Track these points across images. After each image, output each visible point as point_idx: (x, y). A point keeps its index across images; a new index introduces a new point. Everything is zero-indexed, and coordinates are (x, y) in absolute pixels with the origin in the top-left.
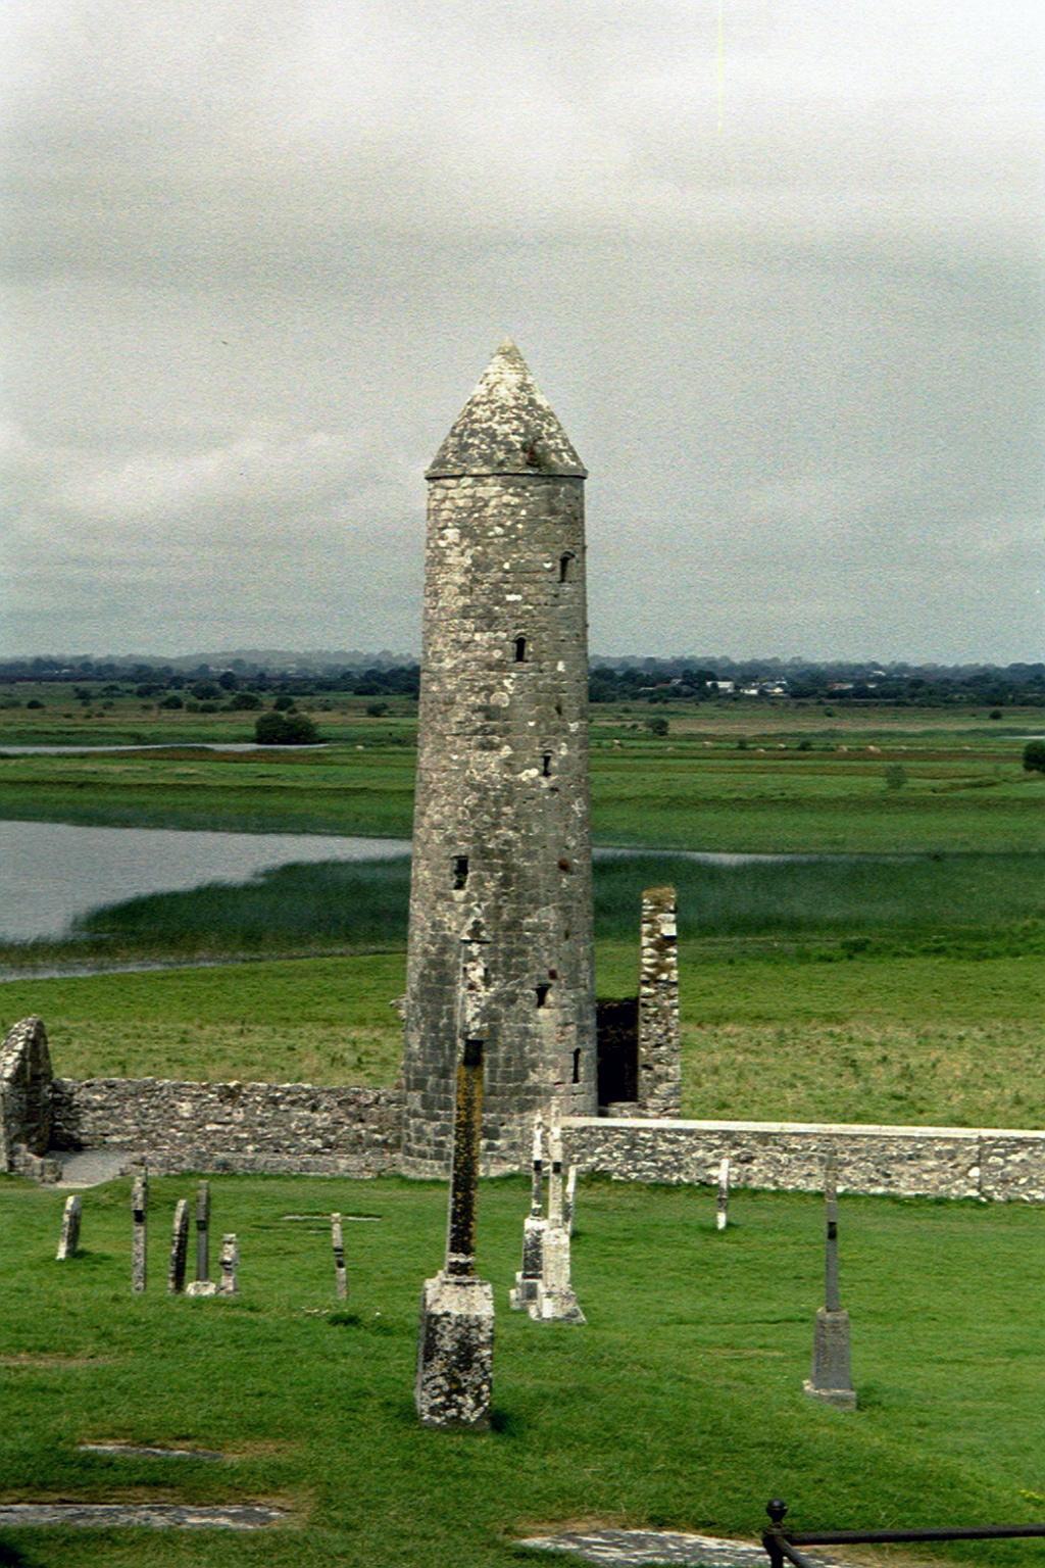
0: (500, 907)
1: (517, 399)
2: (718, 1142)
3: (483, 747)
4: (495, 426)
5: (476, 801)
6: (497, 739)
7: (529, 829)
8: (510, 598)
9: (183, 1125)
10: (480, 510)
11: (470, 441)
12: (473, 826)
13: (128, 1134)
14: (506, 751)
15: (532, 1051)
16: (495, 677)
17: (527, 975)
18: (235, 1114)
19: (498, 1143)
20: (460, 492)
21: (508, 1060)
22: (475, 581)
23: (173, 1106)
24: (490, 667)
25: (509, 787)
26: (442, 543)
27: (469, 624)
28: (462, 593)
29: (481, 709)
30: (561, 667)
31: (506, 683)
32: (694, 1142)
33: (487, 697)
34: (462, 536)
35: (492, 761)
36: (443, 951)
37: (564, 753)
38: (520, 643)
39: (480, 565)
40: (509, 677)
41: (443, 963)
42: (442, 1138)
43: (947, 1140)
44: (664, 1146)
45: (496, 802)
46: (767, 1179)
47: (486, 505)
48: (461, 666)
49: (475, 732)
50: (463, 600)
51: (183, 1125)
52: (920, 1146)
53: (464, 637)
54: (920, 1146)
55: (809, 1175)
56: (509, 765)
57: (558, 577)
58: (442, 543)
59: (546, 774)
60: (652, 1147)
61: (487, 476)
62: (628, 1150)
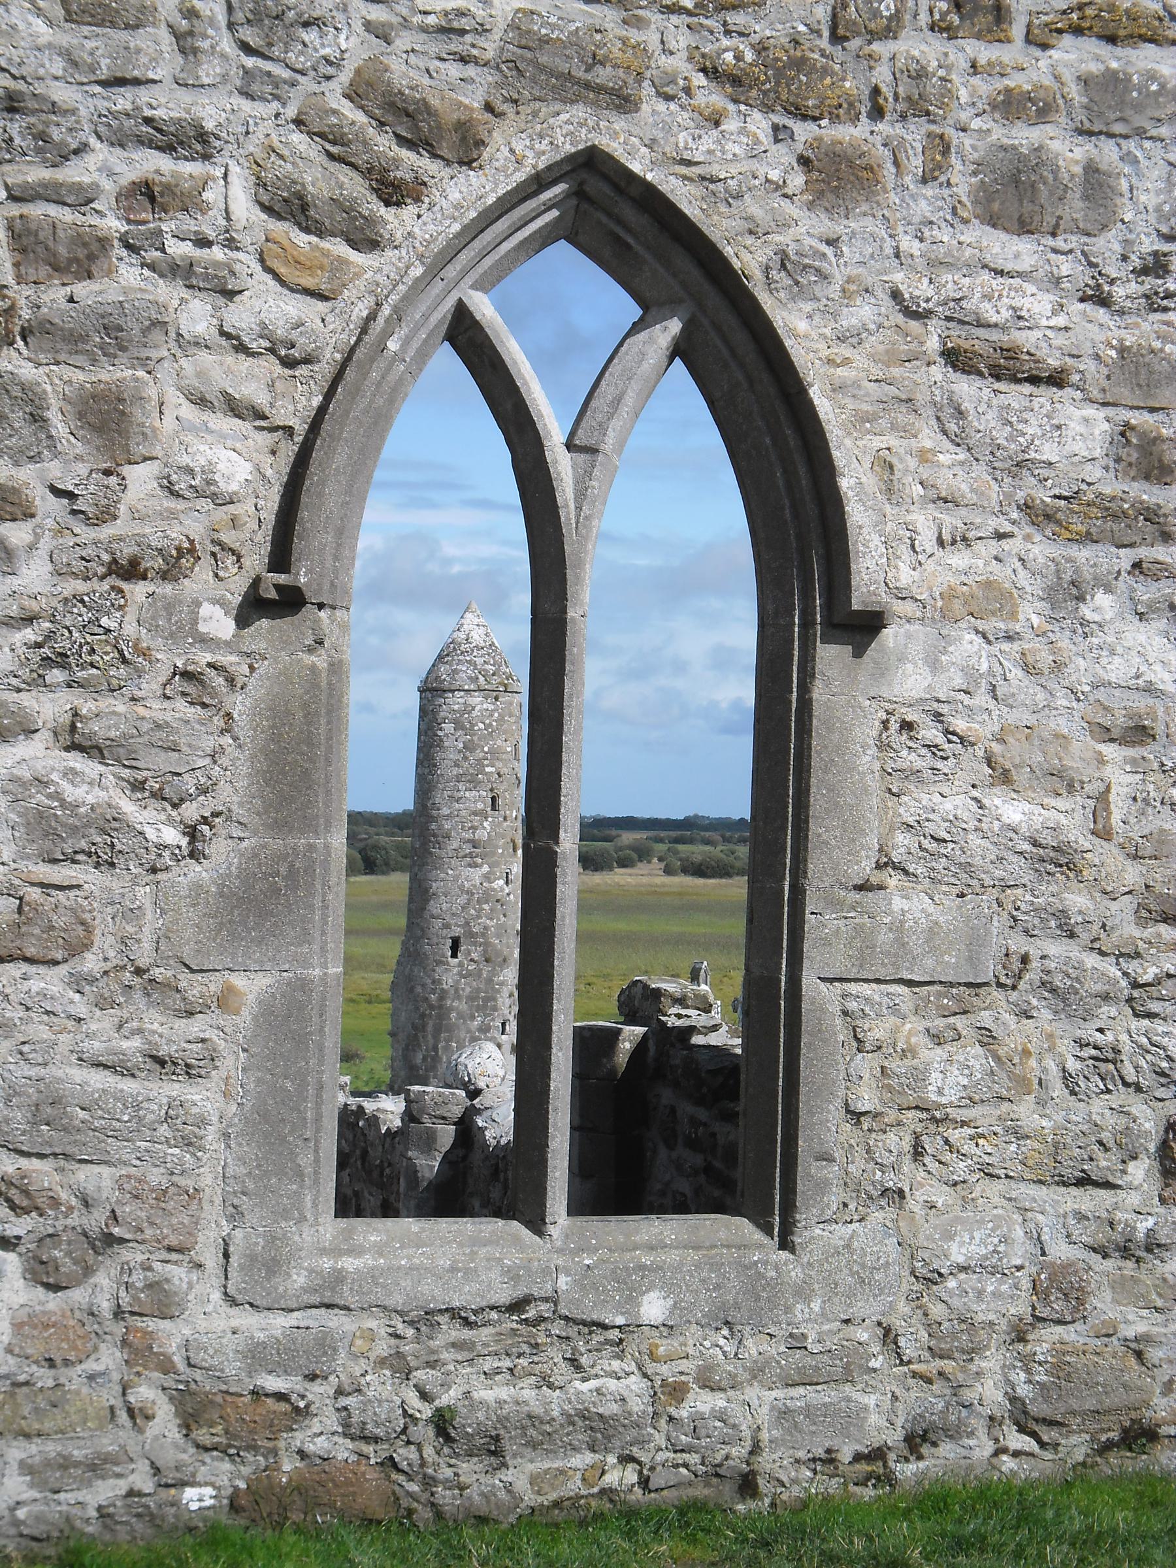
3: (470, 866)
8: (488, 769)
10: (469, 713)
14: (486, 868)
24: (475, 814)
25: (486, 893)
27: (461, 786)
28: (456, 765)
29: (469, 841)
31: (485, 824)
39: (469, 747)
41: (441, 1007)
47: (473, 709)
49: (465, 856)
50: (456, 771)
58: (440, 733)
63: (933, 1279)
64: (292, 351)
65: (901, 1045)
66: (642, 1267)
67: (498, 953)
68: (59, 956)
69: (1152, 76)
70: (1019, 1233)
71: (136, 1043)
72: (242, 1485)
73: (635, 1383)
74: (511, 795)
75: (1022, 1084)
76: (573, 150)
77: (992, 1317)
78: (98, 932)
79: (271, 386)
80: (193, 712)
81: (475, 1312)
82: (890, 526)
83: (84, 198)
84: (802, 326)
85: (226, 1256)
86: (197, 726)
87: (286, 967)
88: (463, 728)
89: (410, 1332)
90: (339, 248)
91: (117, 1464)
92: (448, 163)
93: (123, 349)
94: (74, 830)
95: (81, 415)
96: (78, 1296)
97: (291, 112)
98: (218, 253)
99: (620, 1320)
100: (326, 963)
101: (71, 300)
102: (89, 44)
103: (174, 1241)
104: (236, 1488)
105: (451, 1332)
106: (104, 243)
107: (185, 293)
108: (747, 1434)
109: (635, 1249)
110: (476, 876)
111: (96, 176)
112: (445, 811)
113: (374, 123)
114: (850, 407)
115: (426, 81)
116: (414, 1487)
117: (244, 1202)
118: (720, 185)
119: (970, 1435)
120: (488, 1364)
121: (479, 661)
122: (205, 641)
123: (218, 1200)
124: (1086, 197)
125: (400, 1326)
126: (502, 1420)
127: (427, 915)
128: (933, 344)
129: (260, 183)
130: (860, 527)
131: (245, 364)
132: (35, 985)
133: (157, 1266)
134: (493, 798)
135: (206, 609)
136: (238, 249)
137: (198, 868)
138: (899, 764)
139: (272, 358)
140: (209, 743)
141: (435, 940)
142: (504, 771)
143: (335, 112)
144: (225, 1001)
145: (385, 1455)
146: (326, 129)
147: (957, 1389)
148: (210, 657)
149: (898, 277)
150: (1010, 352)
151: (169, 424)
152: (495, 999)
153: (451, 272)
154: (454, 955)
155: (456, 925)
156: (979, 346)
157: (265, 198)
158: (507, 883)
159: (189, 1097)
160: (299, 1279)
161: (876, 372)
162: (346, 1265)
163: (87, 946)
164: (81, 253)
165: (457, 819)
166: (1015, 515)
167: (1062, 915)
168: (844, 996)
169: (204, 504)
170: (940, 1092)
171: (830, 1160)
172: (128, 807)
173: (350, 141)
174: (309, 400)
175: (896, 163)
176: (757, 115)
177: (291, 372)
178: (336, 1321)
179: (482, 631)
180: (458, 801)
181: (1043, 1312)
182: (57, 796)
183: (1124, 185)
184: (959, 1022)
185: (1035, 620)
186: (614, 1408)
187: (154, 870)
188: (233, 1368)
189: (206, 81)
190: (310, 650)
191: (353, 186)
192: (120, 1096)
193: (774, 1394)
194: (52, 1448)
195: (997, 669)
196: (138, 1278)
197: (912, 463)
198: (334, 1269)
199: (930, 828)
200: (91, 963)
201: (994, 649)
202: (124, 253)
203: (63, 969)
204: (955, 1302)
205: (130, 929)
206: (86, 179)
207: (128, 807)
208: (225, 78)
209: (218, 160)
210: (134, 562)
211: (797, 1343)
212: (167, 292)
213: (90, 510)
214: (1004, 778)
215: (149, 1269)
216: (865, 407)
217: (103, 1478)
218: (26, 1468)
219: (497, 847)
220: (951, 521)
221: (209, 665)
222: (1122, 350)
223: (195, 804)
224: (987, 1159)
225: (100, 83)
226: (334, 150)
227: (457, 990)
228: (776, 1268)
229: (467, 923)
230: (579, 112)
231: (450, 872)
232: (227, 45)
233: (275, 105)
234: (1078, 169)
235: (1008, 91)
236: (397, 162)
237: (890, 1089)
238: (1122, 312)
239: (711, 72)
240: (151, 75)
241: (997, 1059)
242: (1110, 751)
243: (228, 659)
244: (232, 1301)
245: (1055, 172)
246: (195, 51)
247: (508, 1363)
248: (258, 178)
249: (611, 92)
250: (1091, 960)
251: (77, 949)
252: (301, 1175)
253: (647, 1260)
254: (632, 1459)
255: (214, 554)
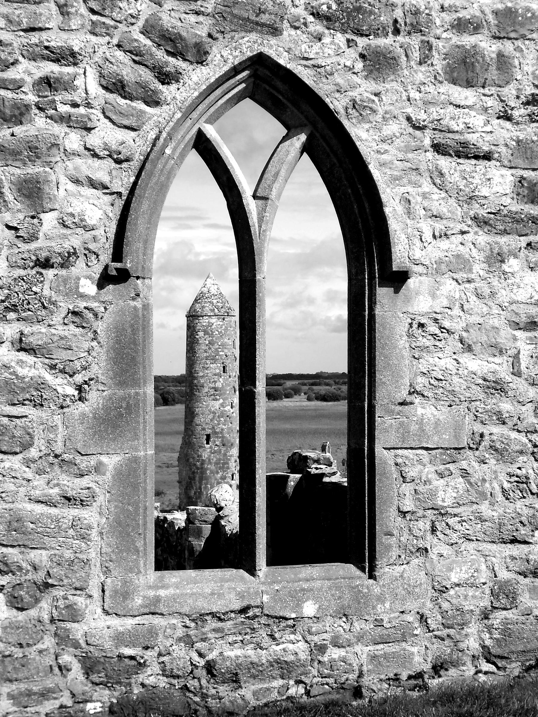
3: (214, 400)
6: (218, 397)
8: (221, 353)
10: (211, 326)
14: (221, 401)
24: (215, 375)
25: (222, 412)
27: (208, 362)
29: (213, 388)
31: (221, 379)
39: (211, 343)
41: (202, 468)
45: (218, 417)
49: (211, 395)
50: (205, 354)
58: (197, 337)
63: (443, 590)
64: (120, 156)
65: (424, 478)
66: (303, 590)
67: (229, 441)
68: (18, 451)
69: (528, 10)
70: (483, 567)
71: (56, 490)
72: (115, 701)
73: (302, 645)
74: (232, 365)
75: (483, 495)
76: (251, 55)
77: (472, 608)
78: (36, 438)
79: (110, 173)
80: (78, 331)
81: (224, 614)
82: (410, 230)
83: (17, 86)
84: (364, 135)
85: (103, 591)
86: (80, 338)
87: (127, 451)
88: (208, 334)
89: (193, 625)
90: (140, 105)
91: (54, 693)
92: (191, 63)
93: (38, 158)
94: (23, 389)
95: (19, 190)
96: (33, 613)
97: (115, 41)
98: (82, 110)
99: (293, 616)
100: (146, 449)
101: (13, 135)
102: (17, 12)
103: (78, 585)
104: (112, 703)
105: (212, 624)
106: (27, 107)
107: (67, 130)
108: (356, 668)
109: (299, 581)
110: (216, 405)
111: (22, 75)
112: (201, 374)
113: (155, 45)
114: (389, 173)
115: (179, 24)
116: (197, 699)
117: (111, 565)
118: (323, 69)
119: (464, 664)
120: (231, 639)
121: (215, 301)
122: (83, 296)
123: (98, 565)
124: (498, 69)
125: (188, 622)
126: (239, 665)
127: (194, 424)
128: (427, 142)
129: (102, 76)
130: (396, 231)
131: (97, 163)
132: (7, 464)
133: (70, 597)
134: (224, 367)
135: (83, 281)
136: (92, 108)
137: (83, 405)
138: (418, 344)
139: (110, 160)
140: (86, 345)
141: (198, 436)
142: (229, 354)
143: (136, 40)
144: (98, 469)
145: (183, 684)
146: (132, 49)
147: (456, 643)
148: (85, 304)
149: (409, 110)
150: (465, 144)
151: (62, 192)
152: (228, 463)
153: (195, 115)
154: (208, 443)
155: (208, 428)
156: (449, 142)
157: (104, 83)
158: (232, 408)
159: (83, 515)
160: (139, 601)
161: (401, 156)
162: (161, 594)
163: (31, 445)
164: (17, 112)
166: (470, 222)
167: (499, 414)
168: (396, 456)
169: (80, 231)
170: (443, 501)
171: (392, 535)
172: (48, 377)
173: (144, 54)
174: (129, 179)
175: (407, 56)
176: (339, 35)
177: (119, 166)
178: (157, 620)
179: (216, 287)
180: (207, 369)
181: (497, 605)
182: (14, 373)
183: (516, 62)
184: (451, 466)
185: (482, 273)
186: (292, 658)
187: (62, 407)
188: (108, 645)
189: (74, 28)
190: (133, 299)
191: (146, 75)
192: (50, 516)
193: (369, 648)
194: (23, 686)
195: (464, 297)
196: (61, 603)
197: (419, 199)
198: (155, 596)
199: (434, 374)
200: (33, 453)
201: (462, 287)
202: (37, 111)
203: (20, 456)
204: (454, 601)
205: (52, 436)
206: (18, 77)
207: (48, 377)
208: (83, 26)
209: (81, 65)
210: (47, 260)
211: (379, 623)
212: (59, 129)
213: (25, 236)
214: (469, 349)
215: (66, 599)
216: (396, 173)
217: (48, 700)
218: (10, 696)
219: (227, 390)
220: (439, 226)
221: (85, 308)
222: (518, 142)
223: (80, 375)
224: (467, 532)
225: (23, 30)
226: (136, 58)
227: (209, 460)
228: (368, 588)
229: (213, 428)
230: (253, 36)
232: (83, 10)
233: (107, 38)
234: (494, 56)
235: (459, 19)
236: (167, 63)
237: (419, 500)
238: (517, 123)
239: (316, 15)
240: (47, 26)
241: (470, 484)
242: (519, 334)
243: (94, 305)
244: (107, 613)
245: (483, 57)
246: (68, 13)
247: (240, 638)
248: (100, 73)
249: (268, 26)
250: (514, 435)
251: (26, 446)
252: (138, 551)
253: (305, 586)
254: (301, 682)
255: (85, 255)
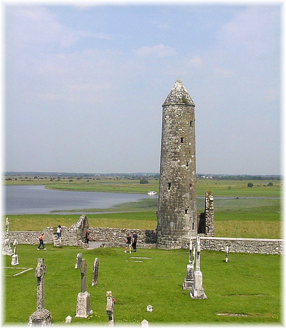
0: (177, 193)
1: (181, 90)
2: (223, 242)
4: (176, 95)
5: (172, 171)
7: (183, 177)
8: (179, 129)
9: (114, 237)
11: (171, 98)
12: (172, 177)
13: (104, 238)
15: (184, 223)
16: (176, 146)
17: (183, 207)
18: (124, 235)
19: (176, 242)
20: (169, 109)
21: (179, 225)
22: (172, 126)
23: (112, 233)
25: (179, 168)
26: (166, 119)
27: (171, 135)
29: (173, 152)
30: (190, 144)
31: (179, 147)
32: (218, 242)
33: (175, 150)
34: (170, 117)
35: (176, 163)
36: (165, 202)
37: (191, 161)
38: (182, 139)
40: (179, 146)
41: (166, 205)
42: (165, 241)
43: (271, 242)
44: (212, 243)
46: (233, 250)
47: (175, 111)
48: (170, 144)
51: (114, 237)
52: (266, 243)
53: (170, 138)
54: (266, 243)
55: (242, 249)
56: (179, 164)
57: (190, 126)
58: (166, 119)
59: (187, 166)
60: (209, 243)
61: (175, 105)
62: (204, 244)
121: (178, 96)
154: (169, 189)
165: (170, 145)
229: (173, 178)
231: (168, 162)
